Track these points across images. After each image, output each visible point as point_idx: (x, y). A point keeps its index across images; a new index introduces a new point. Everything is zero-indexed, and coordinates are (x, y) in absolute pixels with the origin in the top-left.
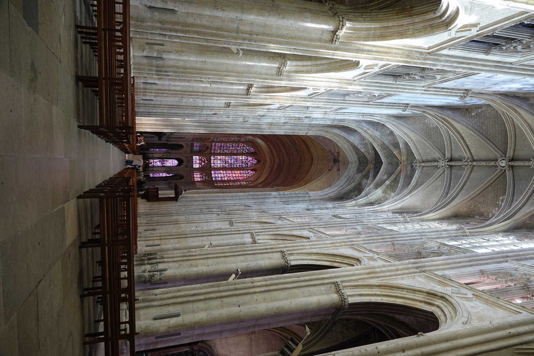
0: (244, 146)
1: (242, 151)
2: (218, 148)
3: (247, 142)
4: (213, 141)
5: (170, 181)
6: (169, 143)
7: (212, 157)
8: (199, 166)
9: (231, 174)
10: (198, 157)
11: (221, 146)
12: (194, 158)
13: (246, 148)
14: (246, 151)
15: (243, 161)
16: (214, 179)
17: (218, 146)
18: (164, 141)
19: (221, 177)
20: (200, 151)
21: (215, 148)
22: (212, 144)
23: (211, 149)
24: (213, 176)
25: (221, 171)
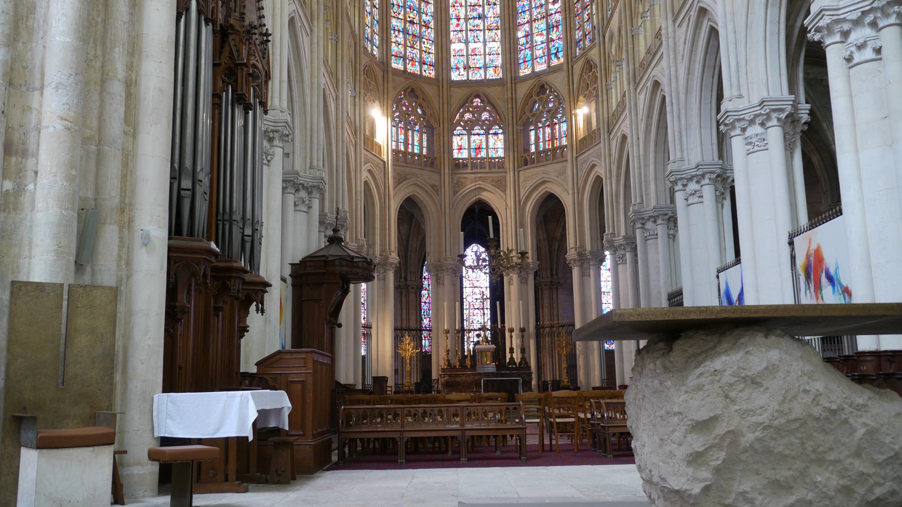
4: (385, 64)
5: (571, 254)
6: (394, 257)
7: (455, 76)
8: (496, 134)
10: (456, 141)
11: (405, 32)
12: (460, 156)
16: (555, 62)
17: (405, 46)
18: (384, 279)
19: (549, 28)
20: (429, 129)
21: (412, 60)
22: (396, 71)
23: (420, 77)
24: (541, 67)
25: (520, 34)
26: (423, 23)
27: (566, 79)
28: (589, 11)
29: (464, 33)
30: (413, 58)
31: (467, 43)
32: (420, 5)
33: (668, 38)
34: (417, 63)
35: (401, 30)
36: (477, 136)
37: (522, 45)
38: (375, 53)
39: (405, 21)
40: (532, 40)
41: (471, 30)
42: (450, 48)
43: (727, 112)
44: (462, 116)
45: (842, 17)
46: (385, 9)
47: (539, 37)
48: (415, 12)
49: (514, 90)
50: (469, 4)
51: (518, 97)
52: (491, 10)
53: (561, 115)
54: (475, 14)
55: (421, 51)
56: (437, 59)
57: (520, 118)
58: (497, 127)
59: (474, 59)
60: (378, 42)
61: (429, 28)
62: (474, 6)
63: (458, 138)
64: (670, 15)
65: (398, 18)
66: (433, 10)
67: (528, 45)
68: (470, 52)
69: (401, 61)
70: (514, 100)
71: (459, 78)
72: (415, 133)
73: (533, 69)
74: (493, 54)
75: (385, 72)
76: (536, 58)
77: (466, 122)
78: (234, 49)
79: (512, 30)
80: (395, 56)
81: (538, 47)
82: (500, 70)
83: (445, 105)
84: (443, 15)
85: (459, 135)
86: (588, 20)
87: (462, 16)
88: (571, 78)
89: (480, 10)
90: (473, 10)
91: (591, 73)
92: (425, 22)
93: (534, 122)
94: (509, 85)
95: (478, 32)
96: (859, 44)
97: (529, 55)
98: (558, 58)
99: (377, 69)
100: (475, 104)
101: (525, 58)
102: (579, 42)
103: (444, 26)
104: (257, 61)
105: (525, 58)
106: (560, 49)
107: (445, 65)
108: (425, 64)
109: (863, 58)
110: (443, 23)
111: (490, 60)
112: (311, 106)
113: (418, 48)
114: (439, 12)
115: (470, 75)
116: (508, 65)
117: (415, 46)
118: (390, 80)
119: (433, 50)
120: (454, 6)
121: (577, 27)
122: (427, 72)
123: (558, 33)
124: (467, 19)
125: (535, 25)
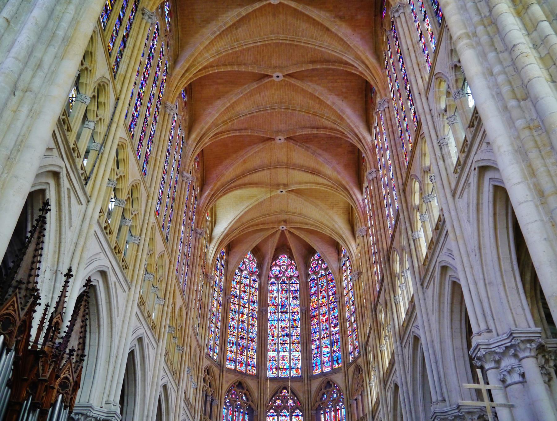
0: (240, 283)
1: (253, 290)
2: (242, 354)
3: (227, 270)
4: (221, 366)
7: (270, 374)
8: (297, 416)
9: (322, 318)
11: (237, 344)
13: (245, 278)
14: (255, 281)
15: (283, 290)
16: (336, 366)
17: (237, 353)
19: (332, 343)
21: (241, 364)
22: (229, 370)
23: (245, 374)
25: (313, 347)
26: (249, 339)
27: (344, 378)
28: (356, 333)
29: (277, 345)
30: (241, 361)
31: (278, 352)
32: (248, 327)
33: (398, 355)
34: (244, 365)
35: (235, 343)
36: (284, 417)
37: (314, 354)
38: (215, 358)
39: (238, 337)
40: (321, 351)
41: (281, 344)
42: (267, 355)
43: (435, 413)
44: (275, 402)
45: (493, 349)
46: (224, 329)
47: (325, 349)
48: (245, 331)
49: (309, 385)
50: (280, 327)
51: (312, 390)
52: (295, 331)
53: (341, 403)
54: (284, 333)
55: (247, 357)
56: (258, 363)
57: (314, 405)
58: (298, 411)
59: (283, 363)
60: (218, 351)
61: (253, 342)
62: (284, 328)
63: (271, 418)
64: (398, 339)
65: (233, 335)
66: (256, 330)
67: (319, 354)
68: (280, 358)
69: (233, 364)
70: (309, 392)
71: (272, 376)
72: (241, 414)
73: (322, 370)
74: (296, 360)
75: (221, 371)
76: (324, 363)
77: (277, 407)
78: (41, 368)
79: (308, 344)
80: (230, 360)
81: (325, 356)
82: (300, 371)
83: (262, 395)
84: (263, 334)
85: (272, 416)
86: (356, 339)
87: (276, 334)
88: (347, 377)
89: (288, 331)
90: (283, 331)
91: (359, 375)
92: (251, 338)
93: (323, 408)
94: (306, 381)
95: (286, 345)
96: (508, 370)
97: (319, 361)
98: (338, 363)
99: (215, 369)
100: (283, 394)
101: (316, 363)
102: (351, 353)
103: (263, 341)
104: (70, 375)
105: (316, 363)
106: (339, 358)
107: (263, 366)
108: (249, 365)
109: (513, 381)
110: (263, 338)
111: (293, 363)
112: (150, 398)
113: (245, 355)
114: (261, 331)
115: (280, 374)
116: (306, 368)
117: (243, 354)
118: (224, 376)
119: (255, 357)
120: (271, 328)
121: (350, 343)
122: (251, 371)
123: (338, 347)
124: (278, 336)
125: (323, 341)
